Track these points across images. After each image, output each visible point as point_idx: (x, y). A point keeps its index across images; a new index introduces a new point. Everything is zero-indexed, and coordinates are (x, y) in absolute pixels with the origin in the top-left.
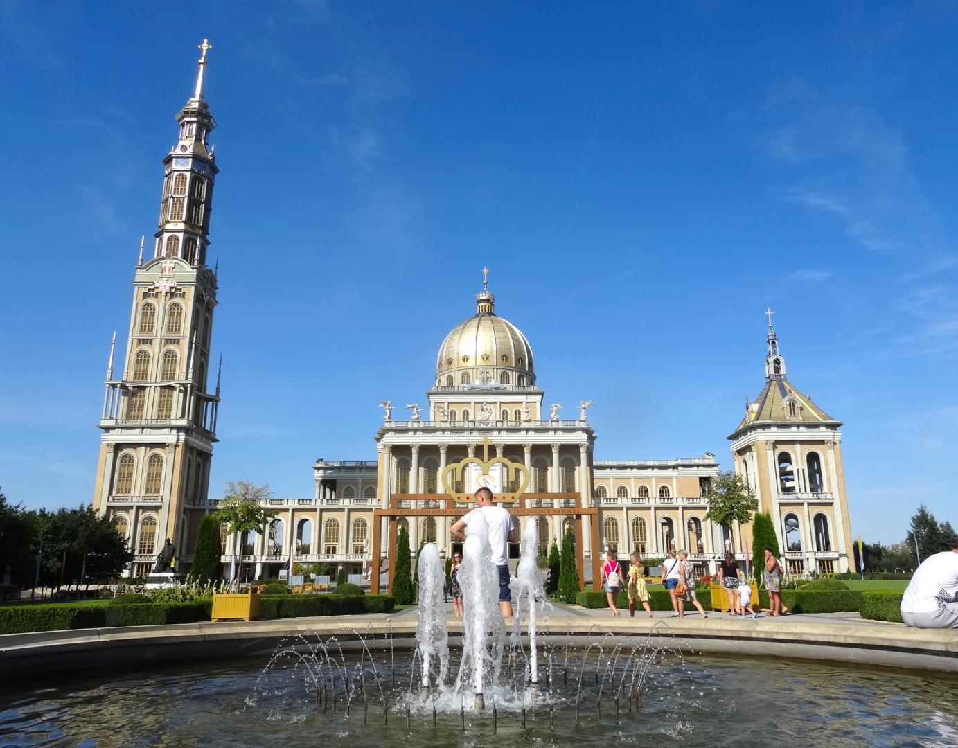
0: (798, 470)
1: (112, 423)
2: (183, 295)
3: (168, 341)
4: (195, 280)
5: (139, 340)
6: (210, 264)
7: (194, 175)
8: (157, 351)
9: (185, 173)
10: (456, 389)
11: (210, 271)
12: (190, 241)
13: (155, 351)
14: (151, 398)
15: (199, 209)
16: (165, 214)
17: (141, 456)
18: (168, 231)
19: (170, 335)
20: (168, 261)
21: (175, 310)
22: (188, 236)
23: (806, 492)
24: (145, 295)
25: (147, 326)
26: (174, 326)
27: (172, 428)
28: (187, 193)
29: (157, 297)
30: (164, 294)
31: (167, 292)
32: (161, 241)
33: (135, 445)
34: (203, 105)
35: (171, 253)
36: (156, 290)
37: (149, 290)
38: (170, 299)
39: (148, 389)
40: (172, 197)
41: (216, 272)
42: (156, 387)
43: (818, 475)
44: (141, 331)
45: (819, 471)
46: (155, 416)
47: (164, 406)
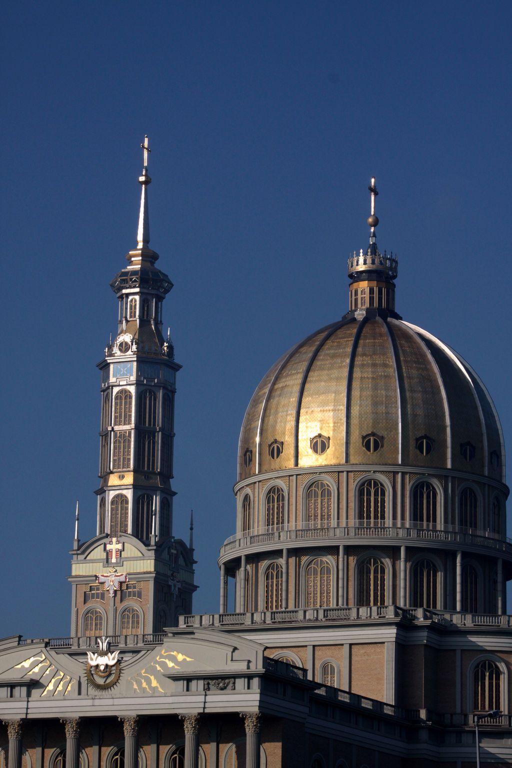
4: (153, 570)
6: (179, 532)
7: (143, 388)
11: (181, 543)
15: (154, 443)
16: (106, 460)
28: (133, 426)
30: (112, 592)
32: (103, 501)
34: (149, 256)
35: (118, 530)
37: (91, 589)
38: (121, 601)
41: (191, 540)
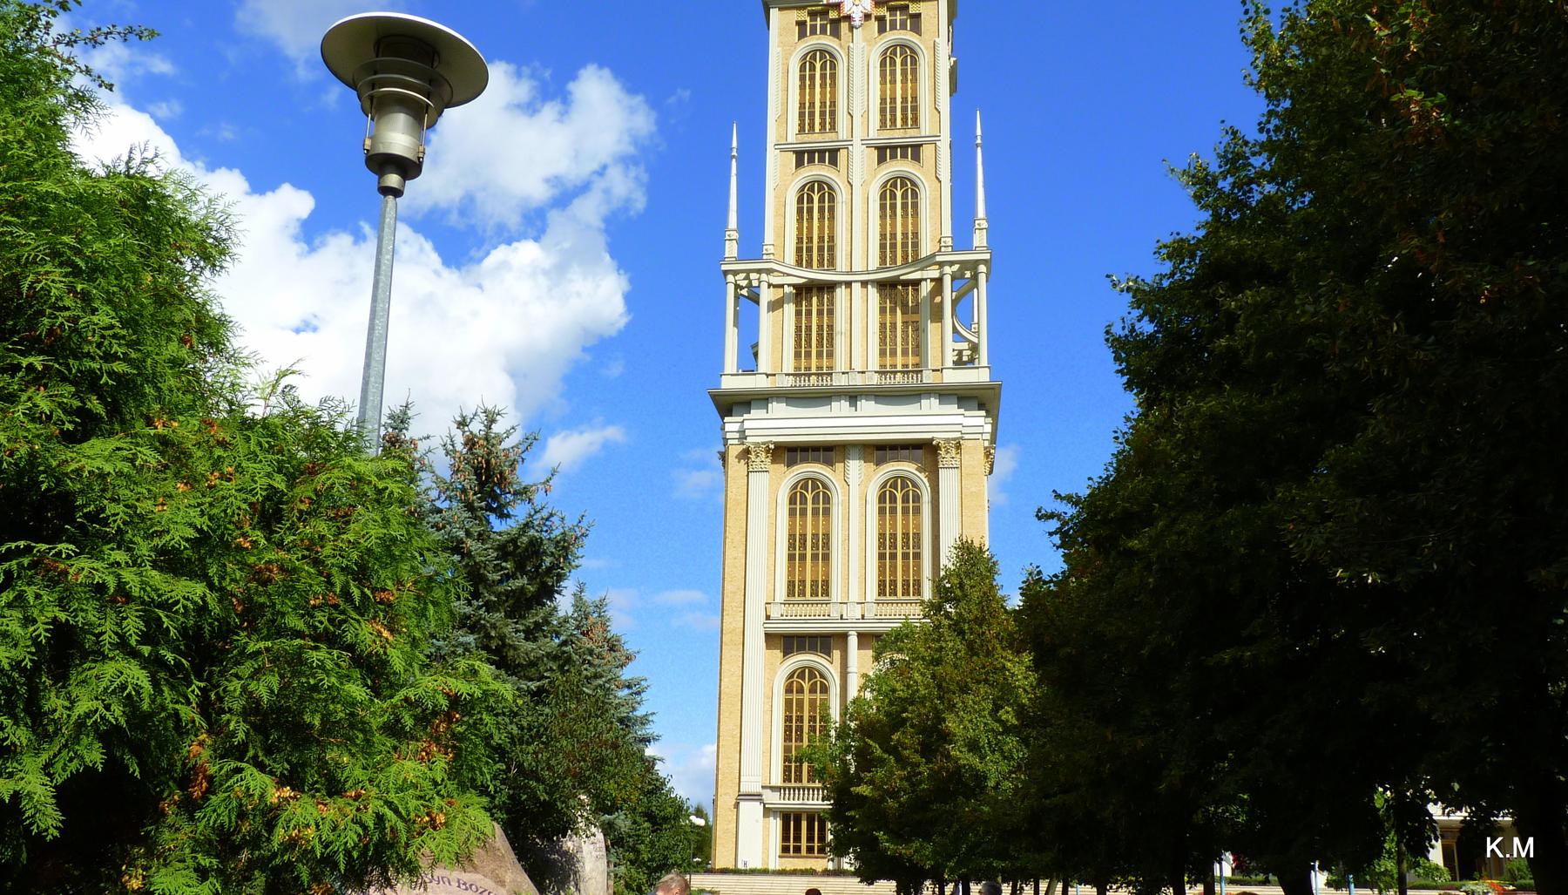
3: (884, 152)
19: (897, 133)
25: (818, 112)
27: (946, 394)
31: (867, 17)
36: (833, 15)
39: (841, 292)
42: (864, 284)
44: (802, 130)
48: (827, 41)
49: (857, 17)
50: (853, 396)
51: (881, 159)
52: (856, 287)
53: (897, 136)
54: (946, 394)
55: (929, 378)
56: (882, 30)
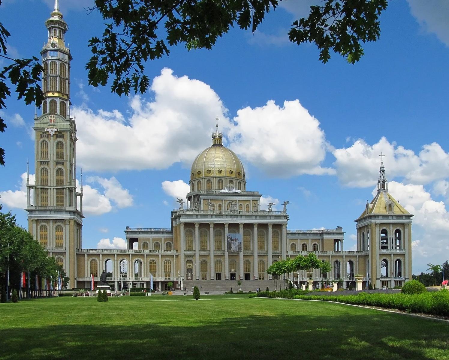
0: (390, 238)
1: (33, 208)
2: (63, 137)
3: (57, 163)
5: (41, 162)
8: (52, 169)
9: (55, 61)
10: (215, 193)
12: (63, 104)
13: (52, 168)
14: (52, 195)
17: (51, 227)
18: (50, 97)
20: (52, 116)
21: (60, 145)
22: (61, 100)
23: (393, 249)
24: (42, 136)
26: (60, 155)
27: (66, 211)
29: (48, 137)
30: (52, 135)
31: (54, 135)
33: (47, 220)
36: (47, 133)
39: (49, 190)
40: (49, 76)
42: (53, 188)
43: (398, 240)
45: (399, 238)
46: (55, 206)
47: (60, 200)
48: (46, 139)
49: (52, 135)
50: (50, 211)
51: (57, 164)
52: (52, 189)
53: (60, 160)
54: (66, 211)
55: (64, 208)
56: (57, 137)
